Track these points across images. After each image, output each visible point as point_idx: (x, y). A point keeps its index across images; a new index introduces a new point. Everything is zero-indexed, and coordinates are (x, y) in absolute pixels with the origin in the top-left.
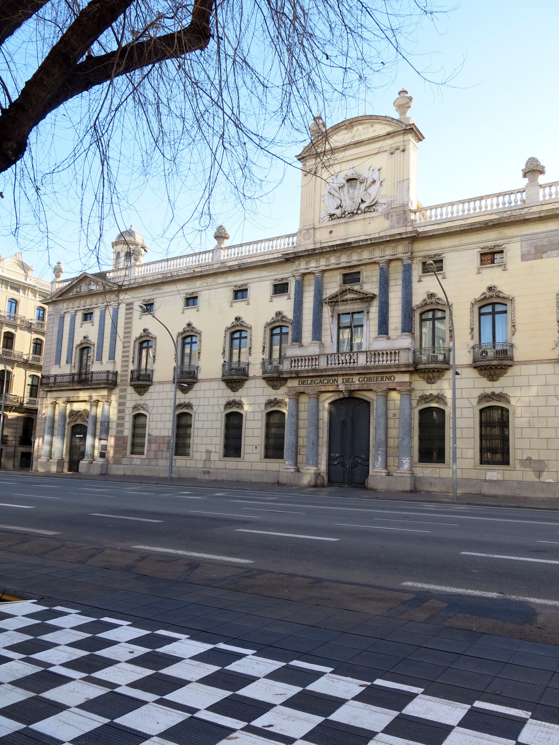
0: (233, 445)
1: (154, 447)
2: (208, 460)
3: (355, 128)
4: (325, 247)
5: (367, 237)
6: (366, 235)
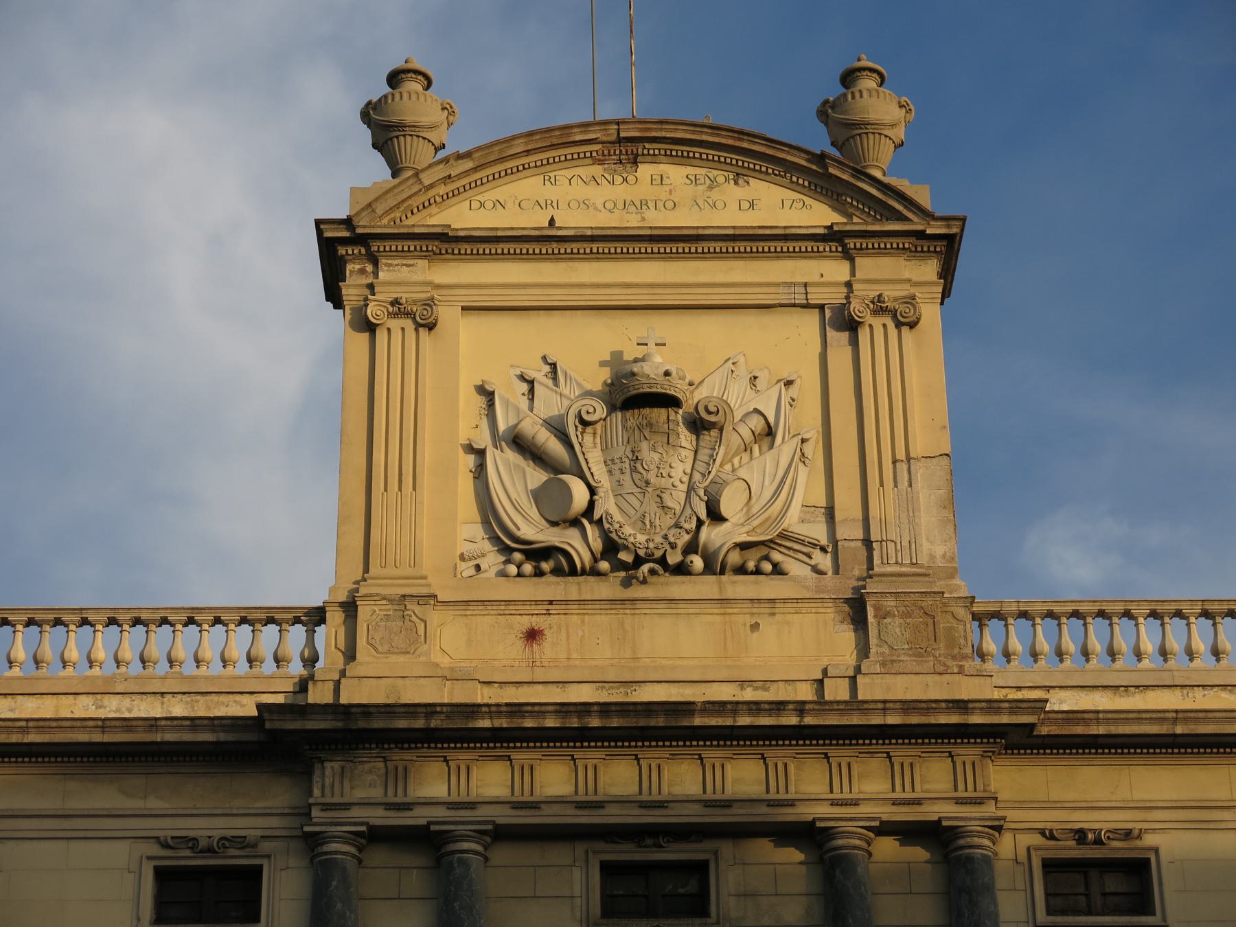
3: (645, 170)
4: (538, 709)
5: (749, 695)
6: (743, 683)
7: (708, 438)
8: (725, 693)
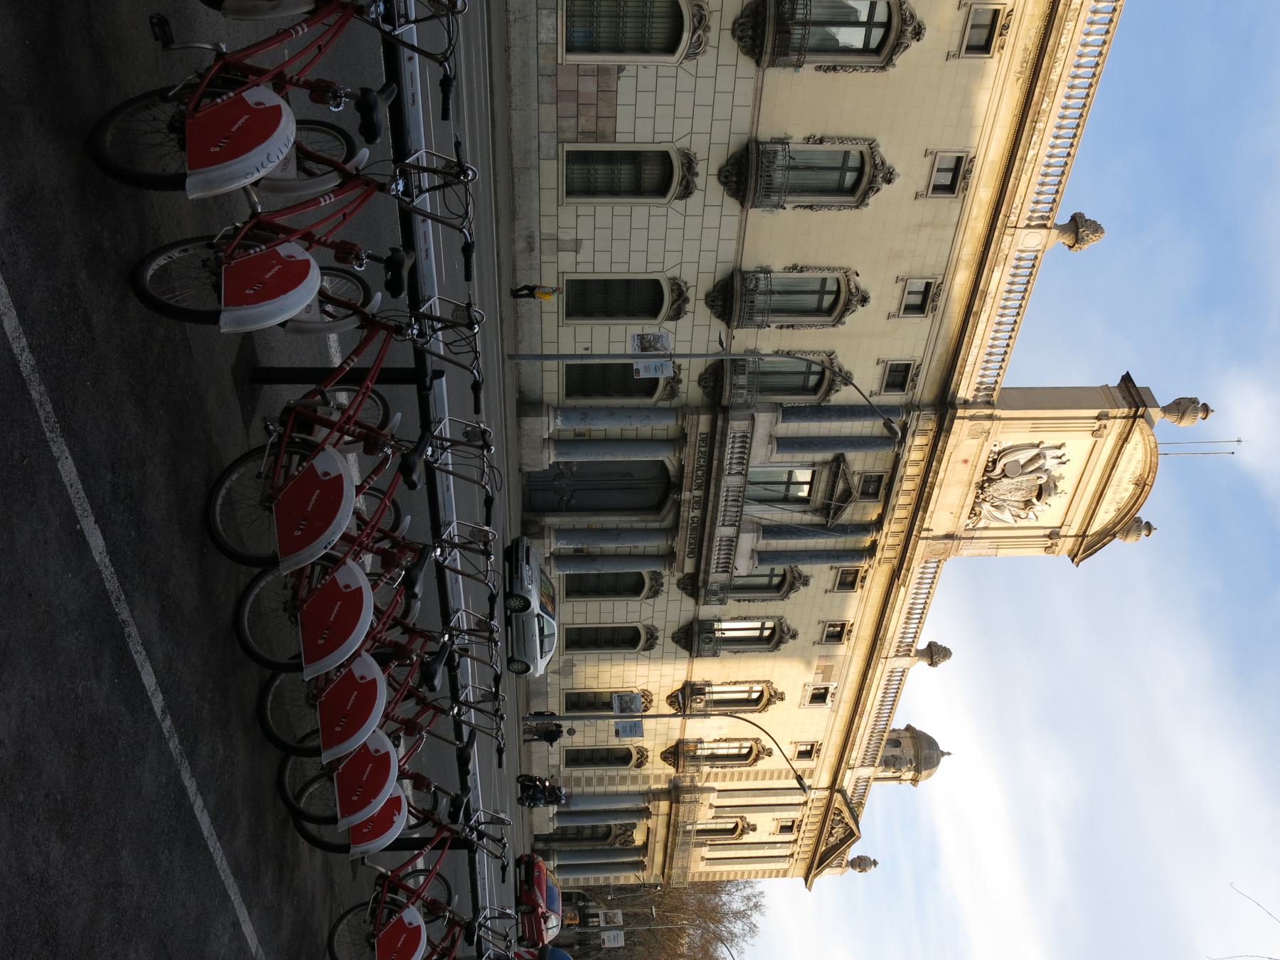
0: (590, 299)
1: (588, 86)
2: (559, 246)
7: (1022, 505)
8: (941, 475)
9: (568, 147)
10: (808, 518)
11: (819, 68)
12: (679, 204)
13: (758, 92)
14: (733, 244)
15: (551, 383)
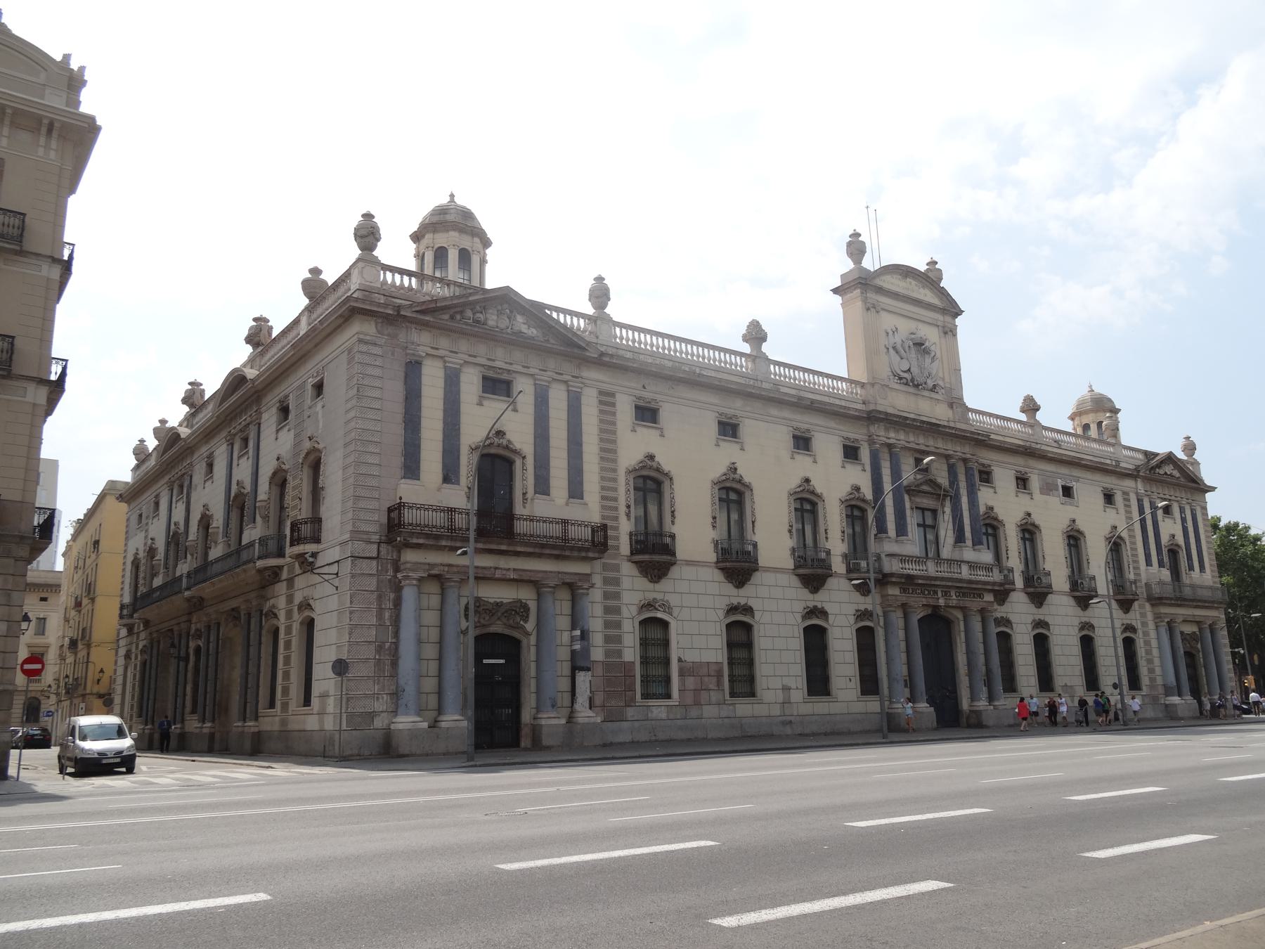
2: (787, 702)
9: (727, 696)
10: (948, 510)
11: (673, 523)
12: (757, 615)
13: (690, 563)
14: (779, 575)
15: (873, 705)
